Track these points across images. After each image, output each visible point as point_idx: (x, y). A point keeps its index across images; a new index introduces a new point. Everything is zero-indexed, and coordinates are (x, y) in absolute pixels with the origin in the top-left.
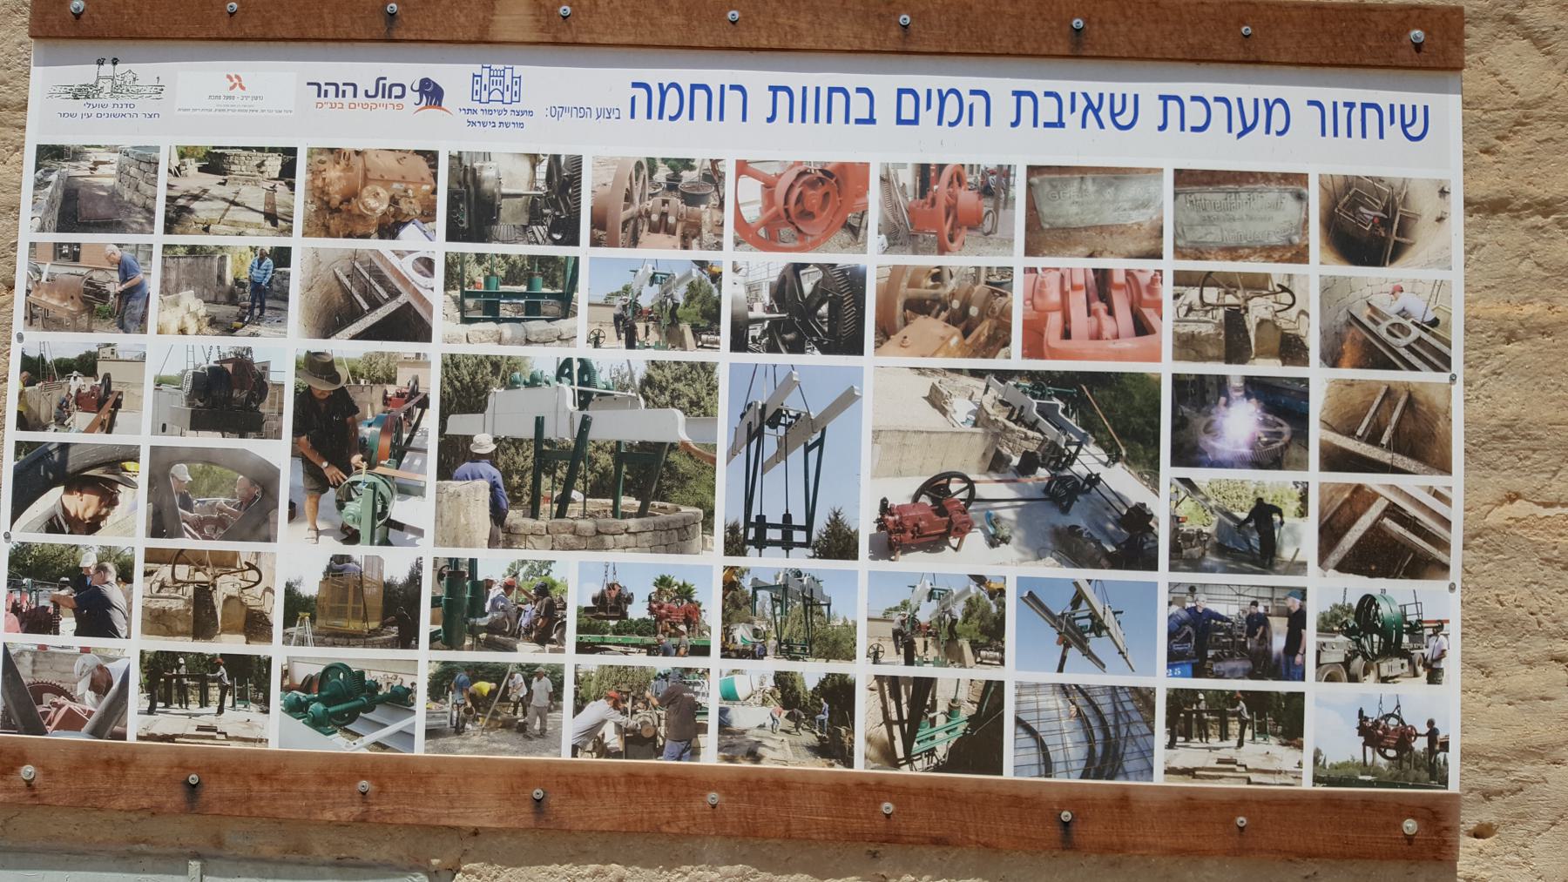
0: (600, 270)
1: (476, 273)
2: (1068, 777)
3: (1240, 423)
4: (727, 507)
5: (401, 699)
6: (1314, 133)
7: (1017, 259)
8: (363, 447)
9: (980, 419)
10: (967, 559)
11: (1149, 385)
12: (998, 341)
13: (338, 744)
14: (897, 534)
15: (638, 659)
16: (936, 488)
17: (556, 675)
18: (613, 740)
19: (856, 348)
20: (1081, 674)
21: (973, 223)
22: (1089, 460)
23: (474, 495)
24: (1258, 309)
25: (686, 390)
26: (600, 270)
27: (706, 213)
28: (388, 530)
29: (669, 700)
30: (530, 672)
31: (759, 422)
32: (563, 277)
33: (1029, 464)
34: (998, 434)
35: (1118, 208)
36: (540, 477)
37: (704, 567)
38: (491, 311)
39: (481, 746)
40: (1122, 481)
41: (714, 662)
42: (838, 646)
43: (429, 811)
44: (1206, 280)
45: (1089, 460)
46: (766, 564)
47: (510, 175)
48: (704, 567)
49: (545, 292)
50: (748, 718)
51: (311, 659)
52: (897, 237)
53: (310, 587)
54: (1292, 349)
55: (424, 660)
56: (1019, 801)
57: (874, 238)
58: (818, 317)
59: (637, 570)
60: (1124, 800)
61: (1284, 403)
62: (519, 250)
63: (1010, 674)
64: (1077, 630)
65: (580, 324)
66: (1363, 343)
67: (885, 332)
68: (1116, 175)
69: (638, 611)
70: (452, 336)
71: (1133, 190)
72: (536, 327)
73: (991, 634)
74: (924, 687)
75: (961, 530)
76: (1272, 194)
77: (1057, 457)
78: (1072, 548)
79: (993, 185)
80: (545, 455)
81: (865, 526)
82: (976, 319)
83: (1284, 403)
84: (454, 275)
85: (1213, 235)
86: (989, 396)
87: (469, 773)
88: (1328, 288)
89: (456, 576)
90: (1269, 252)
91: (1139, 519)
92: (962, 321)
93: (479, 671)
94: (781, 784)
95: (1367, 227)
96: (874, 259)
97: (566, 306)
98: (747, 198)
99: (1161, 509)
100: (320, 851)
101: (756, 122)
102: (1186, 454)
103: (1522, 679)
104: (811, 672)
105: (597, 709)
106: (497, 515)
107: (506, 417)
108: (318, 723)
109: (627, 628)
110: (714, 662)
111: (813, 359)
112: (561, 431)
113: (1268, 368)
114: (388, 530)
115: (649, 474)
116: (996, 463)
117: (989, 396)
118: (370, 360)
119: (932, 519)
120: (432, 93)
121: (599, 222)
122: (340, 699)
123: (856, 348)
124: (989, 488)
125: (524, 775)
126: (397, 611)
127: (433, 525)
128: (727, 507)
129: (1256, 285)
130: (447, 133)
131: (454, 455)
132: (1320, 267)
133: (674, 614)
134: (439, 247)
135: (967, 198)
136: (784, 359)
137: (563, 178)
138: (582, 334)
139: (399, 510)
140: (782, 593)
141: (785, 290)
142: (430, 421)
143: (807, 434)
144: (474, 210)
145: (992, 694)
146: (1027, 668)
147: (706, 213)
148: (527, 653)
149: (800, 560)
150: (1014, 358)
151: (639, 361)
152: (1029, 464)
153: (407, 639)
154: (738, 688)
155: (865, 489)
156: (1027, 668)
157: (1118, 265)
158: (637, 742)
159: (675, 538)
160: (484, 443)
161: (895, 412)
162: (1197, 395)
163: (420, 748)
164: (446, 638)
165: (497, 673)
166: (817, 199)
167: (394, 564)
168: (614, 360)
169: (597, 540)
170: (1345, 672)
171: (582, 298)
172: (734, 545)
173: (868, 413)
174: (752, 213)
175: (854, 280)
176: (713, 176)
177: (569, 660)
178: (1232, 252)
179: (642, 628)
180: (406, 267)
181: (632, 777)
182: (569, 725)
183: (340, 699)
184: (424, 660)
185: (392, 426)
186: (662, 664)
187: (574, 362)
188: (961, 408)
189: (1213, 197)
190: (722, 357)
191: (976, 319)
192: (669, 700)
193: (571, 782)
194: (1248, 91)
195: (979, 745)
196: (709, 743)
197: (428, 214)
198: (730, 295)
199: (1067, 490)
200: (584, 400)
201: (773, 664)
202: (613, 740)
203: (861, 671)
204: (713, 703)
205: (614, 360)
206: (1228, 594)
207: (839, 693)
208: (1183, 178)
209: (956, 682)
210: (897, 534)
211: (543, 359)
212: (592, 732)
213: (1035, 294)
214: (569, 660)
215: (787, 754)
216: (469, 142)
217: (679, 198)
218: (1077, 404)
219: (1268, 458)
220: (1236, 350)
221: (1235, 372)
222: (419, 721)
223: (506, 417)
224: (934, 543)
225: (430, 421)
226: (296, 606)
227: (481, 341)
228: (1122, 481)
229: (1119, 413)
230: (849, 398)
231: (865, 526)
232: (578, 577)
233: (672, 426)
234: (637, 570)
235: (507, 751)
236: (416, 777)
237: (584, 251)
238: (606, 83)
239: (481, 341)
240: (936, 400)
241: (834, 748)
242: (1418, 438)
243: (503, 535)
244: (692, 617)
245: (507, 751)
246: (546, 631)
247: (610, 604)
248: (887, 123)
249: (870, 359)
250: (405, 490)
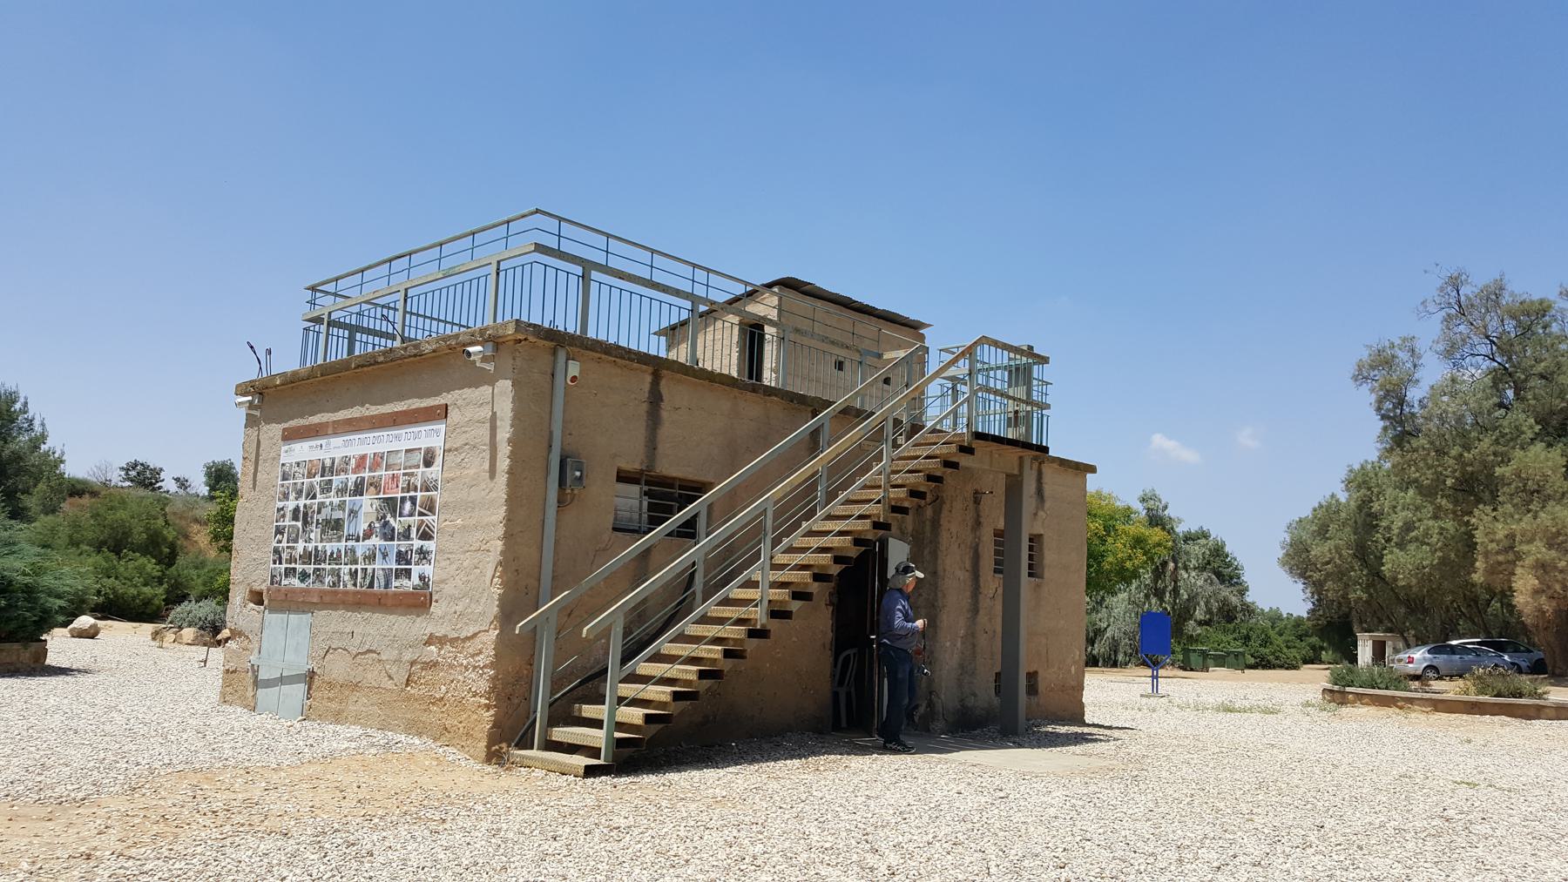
3: (408, 505)
26: (337, 480)
40: (392, 521)
46: (350, 543)
47: (328, 463)
49: (327, 487)
58: (359, 490)
61: (413, 500)
77: (384, 517)
83: (413, 500)
103: (444, 564)
115: (337, 525)
132: (422, 469)
155: (363, 526)
156: (379, 565)
161: (368, 504)
170: (417, 564)
195: (371, 585)
199: (386, 524)
206: (403, 545)
209: (370, 568)
219: (411, 515)
242: (431, 509)
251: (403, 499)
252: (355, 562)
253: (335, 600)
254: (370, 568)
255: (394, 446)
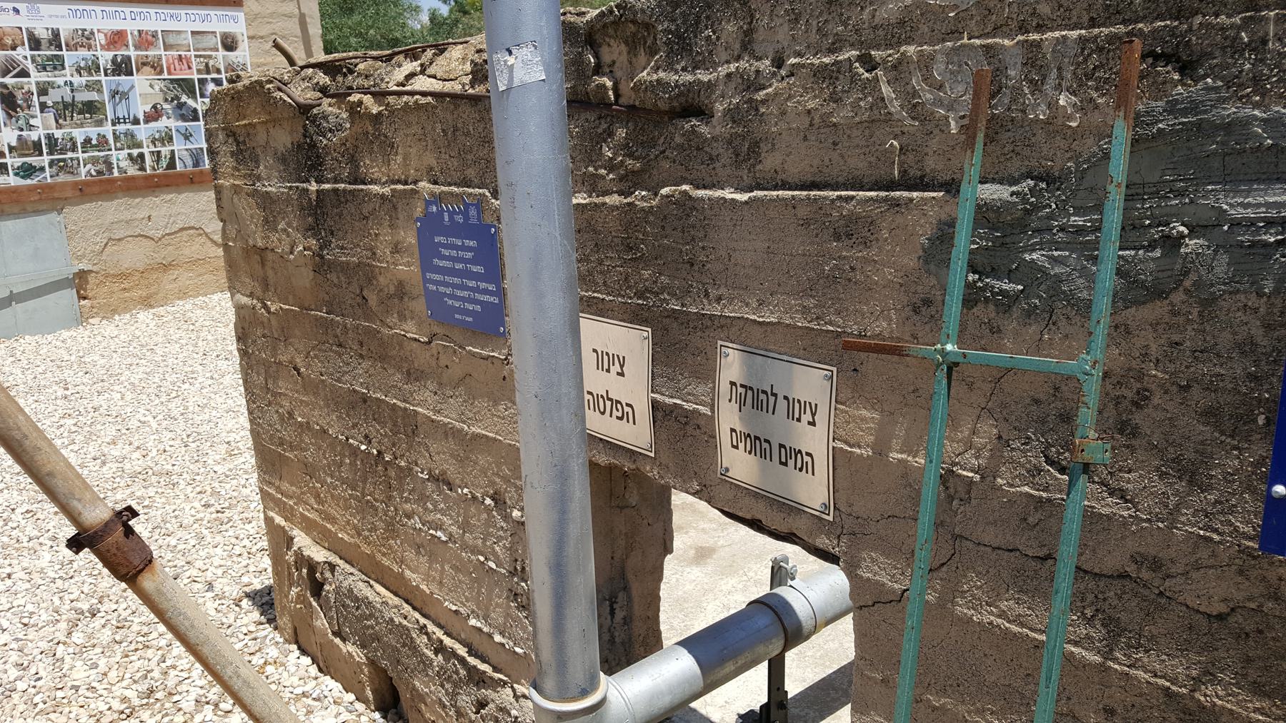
0: (70, 57)
1: (39, 59)
2: (190, 169)
4: (110, 116)
5: (42, 169)
6: (218, 21)
7: (162, 52)
8: (19, 106)
9: (161, 90)
10: (163, 123)
11: (192, 80)
12: (161, 72)
13: (29, 182)
14: (149, 118)
15: (96, 153)
16: (154, 107)
17: (78, 159)
18: (94, 173)
19: (132, 74)
20: (190, 146)
21: (152, 44)
22: (184, 98)
23: (50, 116)
24: (211, 63)
25: (96, 87)
27: (92, 42)
28: (31, 127)
29: (105, 162)
30: (72, 159)
31: (114, 94)
32: (60, 59)
33: (173, 100)
34: (165, 93)
35: (180, 40)
36: (65, 110)
37: (107, 130)
38: (45, 69)
39: (62, 178)
40: (191, 102)
41: (113, 152)
42: (140, 146)
43: (56, 195)
44: (200, 56)
45: (184, 98)
46: (121, 128)
47: (43, 34)
48: (107, 130)
50: (124, 164)
51: (18, 162)
52: (137, 47)
53: (14, 144)
54: (218, 71)
55: (46, 159)
56: (181, 175)
57: (132, 48)
58: (122, 67)
59: (93, 132)
60: (201, 172)
62: (48, 53)
63: (175, 148)
64: (187, 136)
65: (67, 71)
66: (230, 68)
67: (138, 71)
68: (179, 32)
69: (94, 142)
70: (36, 77)
71: (183, 36)
72: (57, 72)
73: (171, 139)
74: (159, 152)
75: (160, 116)
76: (210, 36)
77: (177, 98)
78: (183, 118)
79: (154, 35)
80: (66, 106)
81: (141, 118)
82: (156, 67)
84: (33, 61)
85: (200, 46)
86: (162, 85)
87: (64, 184)
88: (224, 57)
89: (49, 137)
90: (211, 49)
91: (195, 111)
92: (153, 67)
93: (59, 160)
94: (133, 178)
95: (229, 44)
96: (132, 53)
97: (64, 68)
98: (101, 39)
99: (199, 108)
100: (29, 209)
101: (102, 21)
102: (202, 96)
104: (135, 152)
105: (89, 166)
106: (57, 122)
107: (52, 97)
108: (22, 177)
109: (93, 146)
110: (113, 152)
111: (123, 77)
112: (68, 99)
113: (215, 76)
114: (31, 127)
115: (91, 108)
116: (166, 100)
117: (162, 85)
118: (17, 83)
119: (154, 114)
120: (17, 11)
121: (67, 45)
122: (27, 171)
123: (132, 74)
124: (166, 106)
125: (76, 183)
126: (37, 147)
127: (42, 126)
128: (110, 116)
129: (210, 57)
130: (24, 22)
131: (43, 107)
132: (222, 53)
133: (103, 143)
134: (28, 53)
135: (150, 38)
136: (117, 78)
137: (56, 34)
138: (68, 74)
139: (32, 122)
140: (126, 134)
141: (114, 61)
142: (35, 98)
143: (125, 96)
144: (35, 43)
145: (173, 152)
146: (179, 146)
147: (92, 42)
148: (70, 155)
149: (129, 126)
150: (166, 76)
151: (83, 80)
152: (173, 100)
153: (41, 154)
154: (119, 158)
156: (179, 146)
157: (183, 53)
158: (99, 173)
159: (100, 123)
160: (50, 103)
161: (144, 90)
162: (202, 82)
163: (49, 180)
164: (50, 153)
165: (64, 160)
166: (117, 39)
167: (34, 136)
168: (77, 80)
169: (82, 126)
171: (66, 64)
172: (114, 124)
173: (137, 90)
174: (103, 42)
175: (129, 58)
176: (92, 33)
177: (81, 155)
178: (204, 50)
179: (96, 146)
180: (20, 58)
181: (101, 181)
182: (83, 171)
183: (27, 171)
184: (46, 159)
185: (26, 100)
186: (102, 154)
187: (67, 81)
188: (157, 88)
189: (198, 37)
190: (103, 78)
191: (156, 67)
192: (105, 162)
193: (86, 183)
194: (203, 12)
195: (172, 165)
196: (115, 171)
197: (23, 44)
198: (102, 62)
199: (181, 106)
200: (72, 91)
201: (127, 151)
202: (94, 173)
203: (145, 151)
204: (115, 162)
205: (77, 80)
207: (141, 156)
208: (193, 33)
209: (165, 151)
210: (149, 118)
211: (60, 81)
212: (89, 172)
213: (167, 61)
214: (81, 155)
215: (133, 171)
216: (30, 25)
217: (84, 40)
218: (180, 85)
220: (208, 72)
221: (209, 77)
222: (48, 174)
223: (52, 97)
224: (156, 120)
225: (35, 98)
226: (11, 149)
227: (44, 77)
228: (191, 102)
229: (187, 86)
230: (133, 87)
231: (141, 118)
232: (79, 135)
233: (94, 96)
234: (93, 132)
235: (70, 178)
236: (50, 187)
237: (64, 52)
238: (63, 9)
239: (44, 77)
240: (151, 86)
241: (142, 169)
243: (59, 127)
244: (107, 142)
245: (70, 178)
246: (74, 149)
247: (87, 141)
248: (133, 20)
249: (135, 77)
250: (33, 117)
251: (202, 82)
252: (140, 146)
253: (105, 187)
254: (165, 151)
255: (171, 25)
